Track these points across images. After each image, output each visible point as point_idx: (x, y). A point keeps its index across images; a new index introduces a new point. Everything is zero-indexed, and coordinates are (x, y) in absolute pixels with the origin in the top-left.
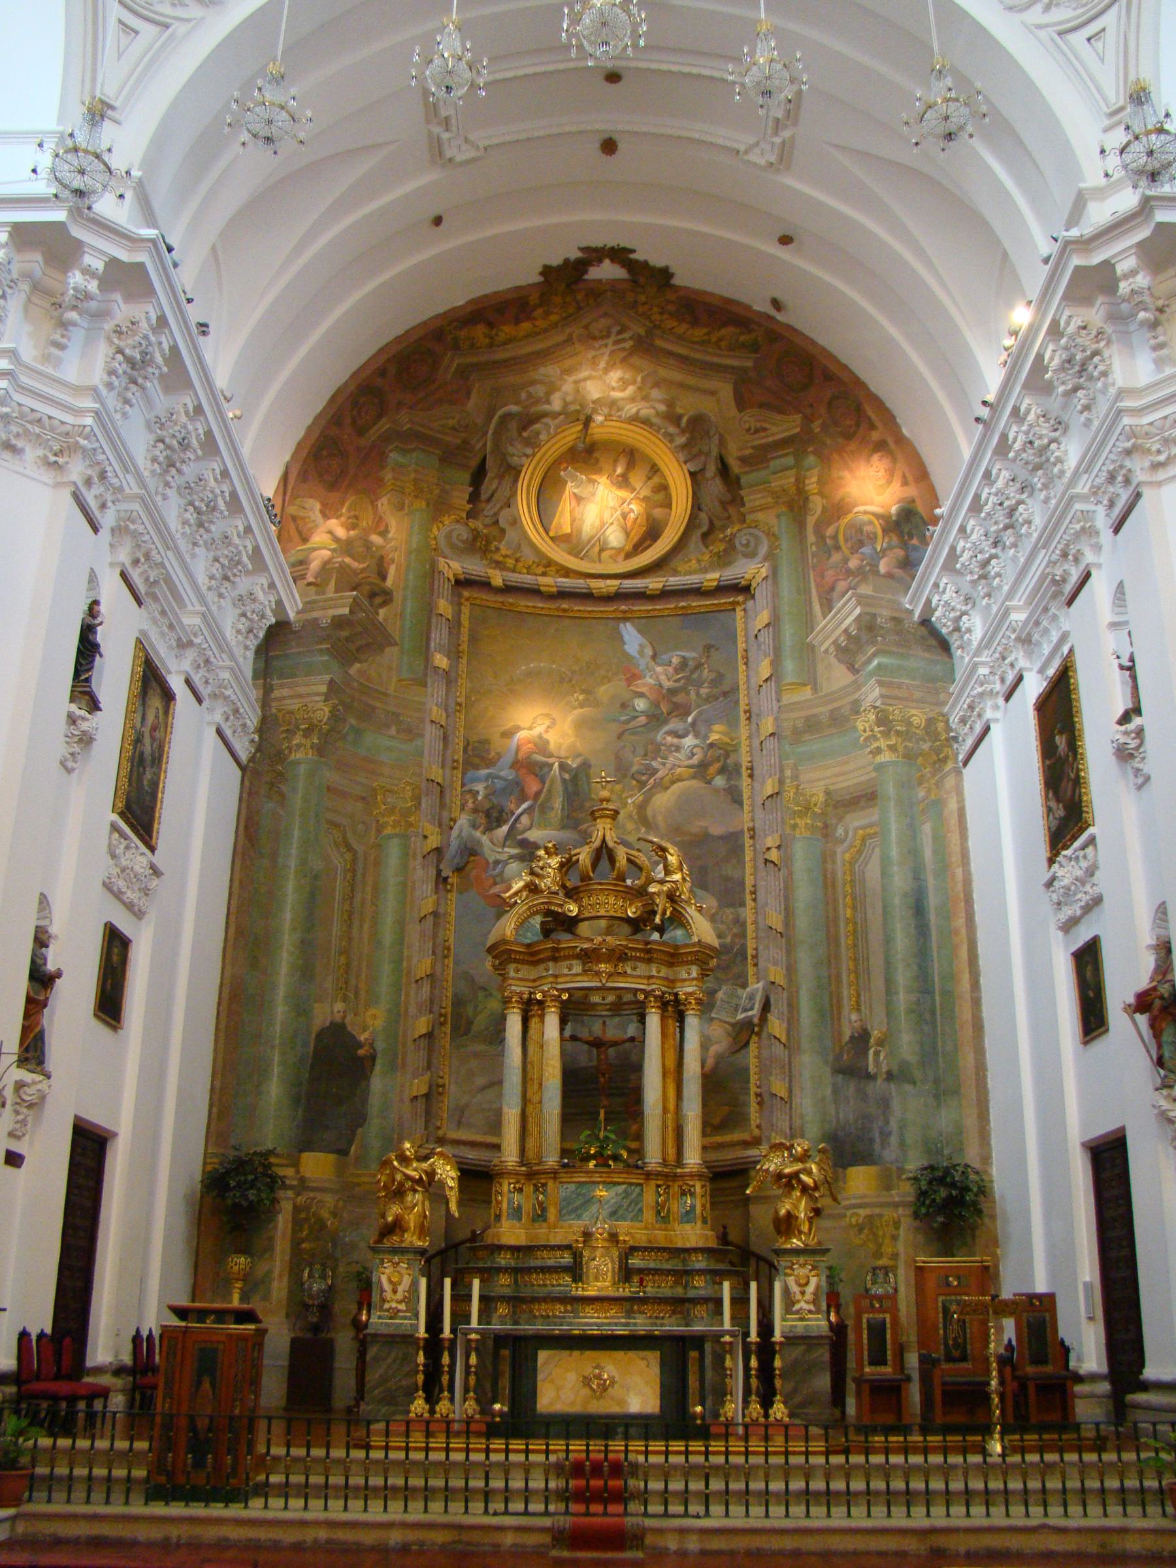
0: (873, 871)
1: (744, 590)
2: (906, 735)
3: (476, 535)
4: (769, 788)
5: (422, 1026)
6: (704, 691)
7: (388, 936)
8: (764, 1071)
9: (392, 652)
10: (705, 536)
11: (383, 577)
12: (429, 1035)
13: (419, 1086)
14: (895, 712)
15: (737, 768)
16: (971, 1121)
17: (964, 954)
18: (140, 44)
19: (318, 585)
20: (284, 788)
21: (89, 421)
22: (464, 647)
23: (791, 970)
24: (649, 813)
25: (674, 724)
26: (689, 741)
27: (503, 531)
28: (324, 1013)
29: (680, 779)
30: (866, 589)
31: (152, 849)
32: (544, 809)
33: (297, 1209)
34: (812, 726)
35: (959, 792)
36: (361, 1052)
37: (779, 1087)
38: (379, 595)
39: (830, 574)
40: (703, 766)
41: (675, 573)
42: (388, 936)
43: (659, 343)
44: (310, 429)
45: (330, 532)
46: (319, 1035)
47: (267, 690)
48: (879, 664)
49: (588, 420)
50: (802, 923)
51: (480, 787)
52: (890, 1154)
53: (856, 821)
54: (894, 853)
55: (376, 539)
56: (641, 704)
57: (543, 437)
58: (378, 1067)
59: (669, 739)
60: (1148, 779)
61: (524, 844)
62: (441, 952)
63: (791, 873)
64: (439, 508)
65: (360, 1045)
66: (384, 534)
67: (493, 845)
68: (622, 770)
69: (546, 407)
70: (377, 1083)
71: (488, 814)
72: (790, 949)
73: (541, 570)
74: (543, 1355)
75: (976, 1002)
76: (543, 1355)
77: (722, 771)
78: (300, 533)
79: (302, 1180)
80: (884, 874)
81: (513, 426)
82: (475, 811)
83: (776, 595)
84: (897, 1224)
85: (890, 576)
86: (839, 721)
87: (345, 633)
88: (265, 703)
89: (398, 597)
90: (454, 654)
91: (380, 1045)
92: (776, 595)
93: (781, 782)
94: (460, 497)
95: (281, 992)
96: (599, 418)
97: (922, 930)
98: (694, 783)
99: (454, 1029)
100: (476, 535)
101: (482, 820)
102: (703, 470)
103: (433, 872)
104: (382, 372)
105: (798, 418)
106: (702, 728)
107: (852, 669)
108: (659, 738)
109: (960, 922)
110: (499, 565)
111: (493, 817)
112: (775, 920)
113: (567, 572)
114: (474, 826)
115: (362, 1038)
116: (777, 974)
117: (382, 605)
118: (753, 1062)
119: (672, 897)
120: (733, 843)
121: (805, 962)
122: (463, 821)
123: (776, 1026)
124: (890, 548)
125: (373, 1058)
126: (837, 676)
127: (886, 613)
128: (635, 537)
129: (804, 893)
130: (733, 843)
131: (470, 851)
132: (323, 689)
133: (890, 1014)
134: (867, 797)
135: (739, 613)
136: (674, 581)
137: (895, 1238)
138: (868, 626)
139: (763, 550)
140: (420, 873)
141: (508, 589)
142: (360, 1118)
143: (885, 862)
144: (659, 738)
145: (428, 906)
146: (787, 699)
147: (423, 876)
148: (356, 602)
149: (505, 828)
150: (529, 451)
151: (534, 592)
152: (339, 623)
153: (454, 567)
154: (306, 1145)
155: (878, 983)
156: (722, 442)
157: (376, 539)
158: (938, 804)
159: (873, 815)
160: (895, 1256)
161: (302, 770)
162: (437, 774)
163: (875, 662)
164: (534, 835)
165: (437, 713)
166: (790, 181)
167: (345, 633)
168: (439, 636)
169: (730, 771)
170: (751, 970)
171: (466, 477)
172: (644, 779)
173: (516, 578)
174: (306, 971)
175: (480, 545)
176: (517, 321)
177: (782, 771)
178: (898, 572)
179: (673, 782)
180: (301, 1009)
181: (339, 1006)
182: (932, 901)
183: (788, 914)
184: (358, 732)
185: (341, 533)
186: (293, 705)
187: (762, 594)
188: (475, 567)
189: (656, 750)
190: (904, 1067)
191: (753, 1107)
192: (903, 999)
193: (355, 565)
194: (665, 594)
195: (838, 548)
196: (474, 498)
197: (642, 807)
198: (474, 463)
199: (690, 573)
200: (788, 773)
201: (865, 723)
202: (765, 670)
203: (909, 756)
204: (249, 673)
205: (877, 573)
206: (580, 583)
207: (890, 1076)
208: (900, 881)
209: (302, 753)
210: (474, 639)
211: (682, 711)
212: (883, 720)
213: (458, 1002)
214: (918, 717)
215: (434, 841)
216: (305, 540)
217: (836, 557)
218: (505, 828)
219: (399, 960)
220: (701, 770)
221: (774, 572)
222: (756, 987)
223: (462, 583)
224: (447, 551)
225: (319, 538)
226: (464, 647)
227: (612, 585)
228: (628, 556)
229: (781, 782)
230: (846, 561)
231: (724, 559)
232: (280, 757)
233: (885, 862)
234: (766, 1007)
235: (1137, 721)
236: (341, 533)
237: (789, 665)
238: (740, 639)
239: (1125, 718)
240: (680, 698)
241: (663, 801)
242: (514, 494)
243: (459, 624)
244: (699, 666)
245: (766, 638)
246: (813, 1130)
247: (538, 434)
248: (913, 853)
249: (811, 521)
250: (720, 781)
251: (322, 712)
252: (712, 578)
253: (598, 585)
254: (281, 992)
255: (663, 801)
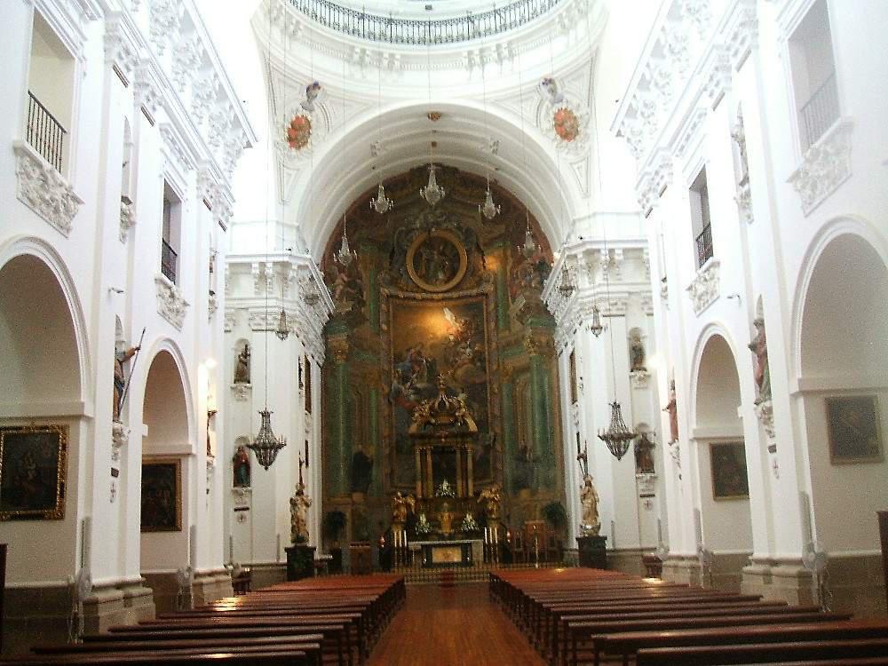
0: (529, 394)
1: (486, 295)
2: (539, 347)
3: (392, 277)
4: (495, 367)
5: (387, 451)
6: (473, 332)
7: (374, 424)
8: (495, 462)
9: (368, 324)
10: (472, 273)
11: (362, 296)
12: (390, 454)
13: (388, 471)
14: (536, 339)
15: (485, 358)
16: (559, 474)
17: (557, 420)
18: (293, 176)
19: (340, 299)
20: (336, 374)
21: (298, 313)
22: (391, 319)
23: (502, 430)
24: (455, 376)
25: (463, 344)
26: (468, 350)
27: (402, 275)
28: (357, 448)
29: (465, 364)
30: (527, 293)
31: (310, 412)
32: (421, 377)
33: (352, 510)
34: (508, 344)
35: (557, 365)
36: (369, 461)
37: (499, 466)
38: (362, 303)
39: (515, 289)
40: (473, 359)
41: (462, 290)
42: (374, 424)
43: (454, 197)
44: (330, 238)
45: (343, 280)
46: (356, 455)
47: (327, 339)
48: (531, 323)
49: (430, 231)
50: (506, 412)
51: (399, 370)
52: (534, 486)
53: (523, 378)
54: (536, 387)
55: (358, 281)
56: (452, 338)
57: (414, 238)
58: (374, 468)
59: (462, 350)
60: (753, 220)
61: (416, 389)
62: (391, 428)
63: (502, 396)
64: (379, 268)
65: (367, 458)
66: (361, 278)
67: (406, 389)
68: (446, 361)
69: (414, 226)
70: (374, 472)
71: (403, 380)
72: (502, 419)
73: (415, 290)
74: (433, 550)
75: (561, 436)
76: (433, 550)
77: (480, 360)
78: (331, 280)
79: (353, 502)
80: (532, 395)
81: (403, 235)
82: (399, 377)
83: (496, 296)
84: (536, 507)
85: (535, 288)
86: (518, 342)
87: (351, 317)
88: (326, 344)
89: (367, 303)
90: (388, 323)
91: (374, 458)
92: (496, 296)
93: (499, 366)
94: (386, 264)
95: (341, 442)
96: (433, 230)
97: (544, 413)
98: (470, 365)
99: (397, 451)
100: (392, 277)
101: (401, 380)
102: (471, 249)
103: (387, 401)
104: (355, 212)
105: (504, 226)
106: (472, 346)
107: (523, 324)
108: (458, 349)
109: (557, 410)
110: (401, 289)
111: (404, 379)
112: (497, 412)
113: (425, 291)
114: (399, 383)
115: (368, 456)
116: (498, 430)
117: (363, 306)
118: (491, 458)
119: (463, 416)
120: (483, 384)
121: (507, 426)
122: (395, 382)
123: (498, 447)
124: (536, 277)
125: (372, 462)
126: (517, 326)
127: (534, 302)
128: (448, 275)
129: (506, 402)
130: (483, 384)
131: (399, 392)
132: (345, 338)
133: (534, 439)
134: (526, 369)
135: (484, 303)
136: (465, 293)
137: (535, 510)
138: (527, 307)
139: (492, 280)
140: (383, 402)
141: (405, 298)
142: (370, 482)
143: (532, 391)
144: (458, 349)
145: (386, 413)
146: (500, 335)
147: (383, 401)
148: (354, 305)
149: (409, 384)
150: (409, 244)
151: (414, 299)
152: (348, 313)
153: (385, 291)
154: (354, 491)
155: (530, 431)
156: (477, 239)
157: (358, 281)
158: (550, 371)
159: (529, 375)
160: (535, 516)
161: (341, 368)
162: (386, 368)
163: (530, 320)
164: (418, 386)
165: (384, 346)
166: (497, 157)
167: (351, 317)
168: (383, 318)
169: (482, 361)
170: (490, 428)
171: (388, 254)
172: (452, 365)
173: (407, 294)
174: (349, 435)
175: (393, 282)
176: (402, 189)
177: (498, 361)
178: (538, 286)
179: (463, 365)
180: (348, 448)
181: (360, 446)
182: (547, 403)
183: (501, 409)
184: (358, 353)
185: (346, 279)
186: (335, 344)
187: (492, 298)
188: (393, 291)
189: (458, 354)
190: (538, 458)
191: (492, 472)
192: (537, 436)
193: (352, 291)
194: (459, 298)
195: (517, 278)
196: (391, 263)
197: (453, 374)
198: (391, 249)
199: (467, 289)
200: (500, 361)
201: (526, 343)
202: (493, 325)
203: (541, 354)
204: (319, 332)
205: (530, 286)
206: (429, 296)
207: (534, 461)
208: (537, 397)
209: (340, 361)
210: (395, 316)
211: (465, 340)
212: (532, 342)
213: (397, 442)
214: (544, 340)
215: (387, 390)
216: (334, 282)
217: (517, 282)
218: (409, 384)
219: (378, 431)
220: (472, 361)
221: (496, 288)
222: (492, 434)
223: (390, 296)
224: (384, 285)
225: (338, 281)
226: (391, 319)
227: (441, 296)
228: (447, 282)
229: (499, 366)
230: (520, 282)
231: (479, 284)
232: (333, 363)
233: (532, 391)
234: (495, 439)
235: (746, 187)
236: (346, 279)
237: (501, 324)
238: (485, 313)
239: (742, 184)
240: (465, 335)
241: (460, 372)
242: (405, 261)
243: (389, 311)
244: (470, 323)
245: (493, 314)
246: (510, 479)
247: (412, 237)
248: (542, 387)
249: (508, 268)
250: (479, 364)
251: (345, 346)
252: (474, 292)
253: (435, 296)
254: (341, 442)
255: (460, 372)
